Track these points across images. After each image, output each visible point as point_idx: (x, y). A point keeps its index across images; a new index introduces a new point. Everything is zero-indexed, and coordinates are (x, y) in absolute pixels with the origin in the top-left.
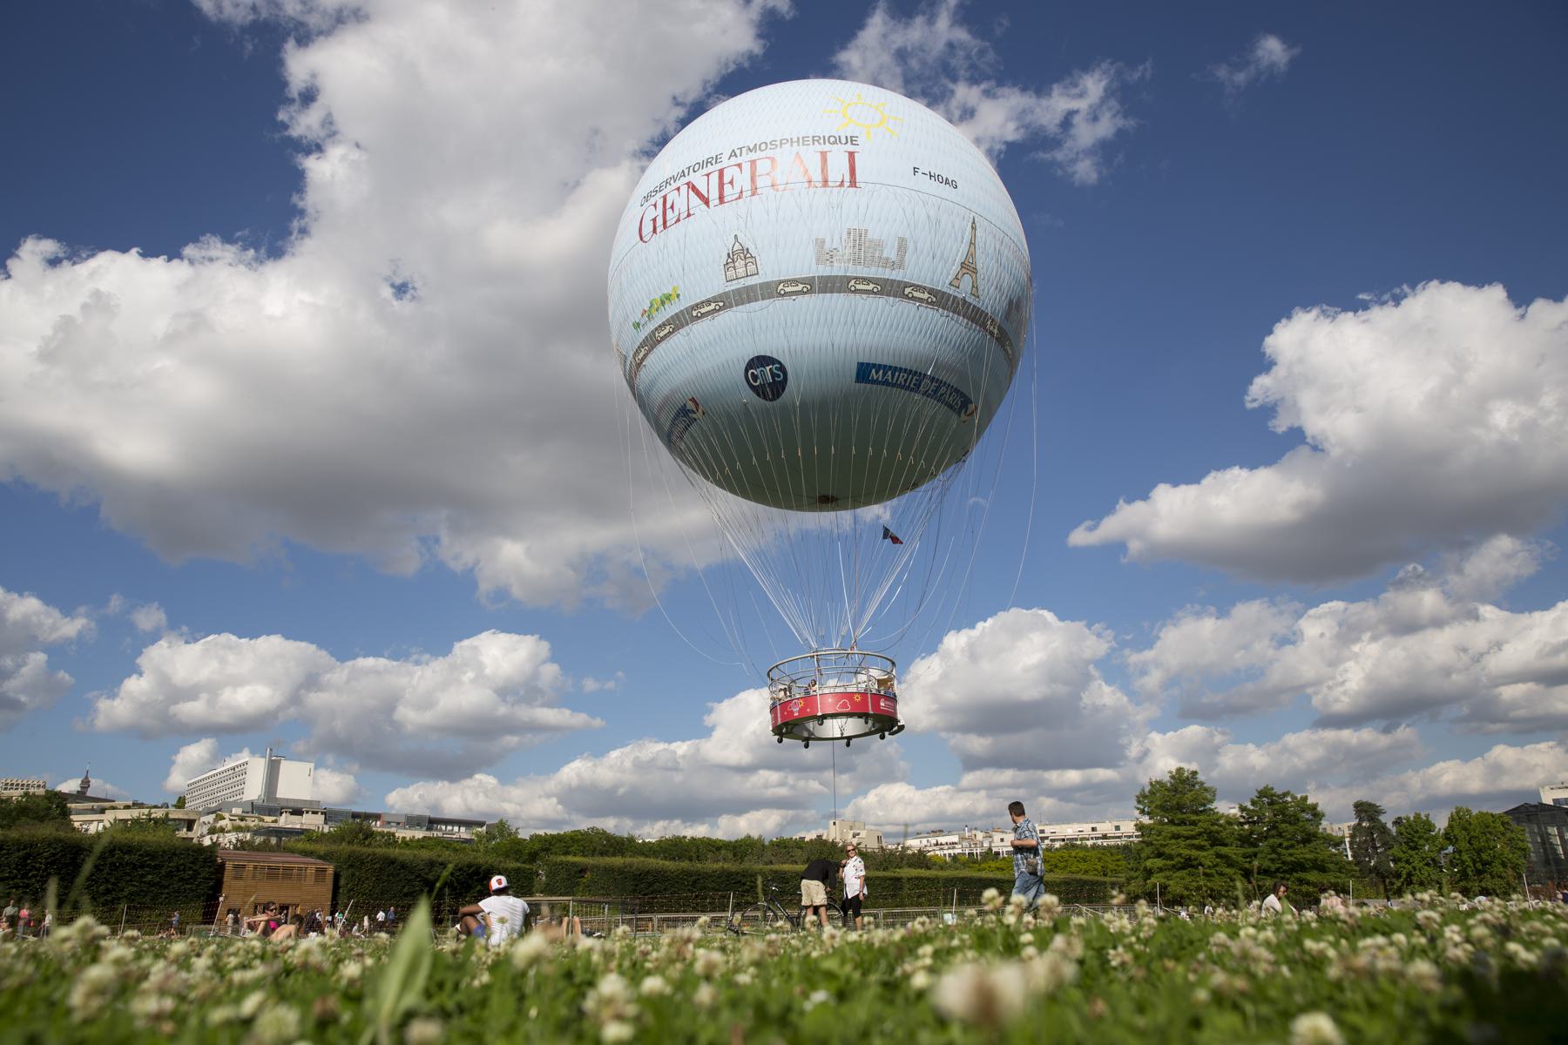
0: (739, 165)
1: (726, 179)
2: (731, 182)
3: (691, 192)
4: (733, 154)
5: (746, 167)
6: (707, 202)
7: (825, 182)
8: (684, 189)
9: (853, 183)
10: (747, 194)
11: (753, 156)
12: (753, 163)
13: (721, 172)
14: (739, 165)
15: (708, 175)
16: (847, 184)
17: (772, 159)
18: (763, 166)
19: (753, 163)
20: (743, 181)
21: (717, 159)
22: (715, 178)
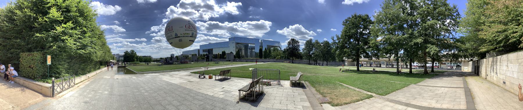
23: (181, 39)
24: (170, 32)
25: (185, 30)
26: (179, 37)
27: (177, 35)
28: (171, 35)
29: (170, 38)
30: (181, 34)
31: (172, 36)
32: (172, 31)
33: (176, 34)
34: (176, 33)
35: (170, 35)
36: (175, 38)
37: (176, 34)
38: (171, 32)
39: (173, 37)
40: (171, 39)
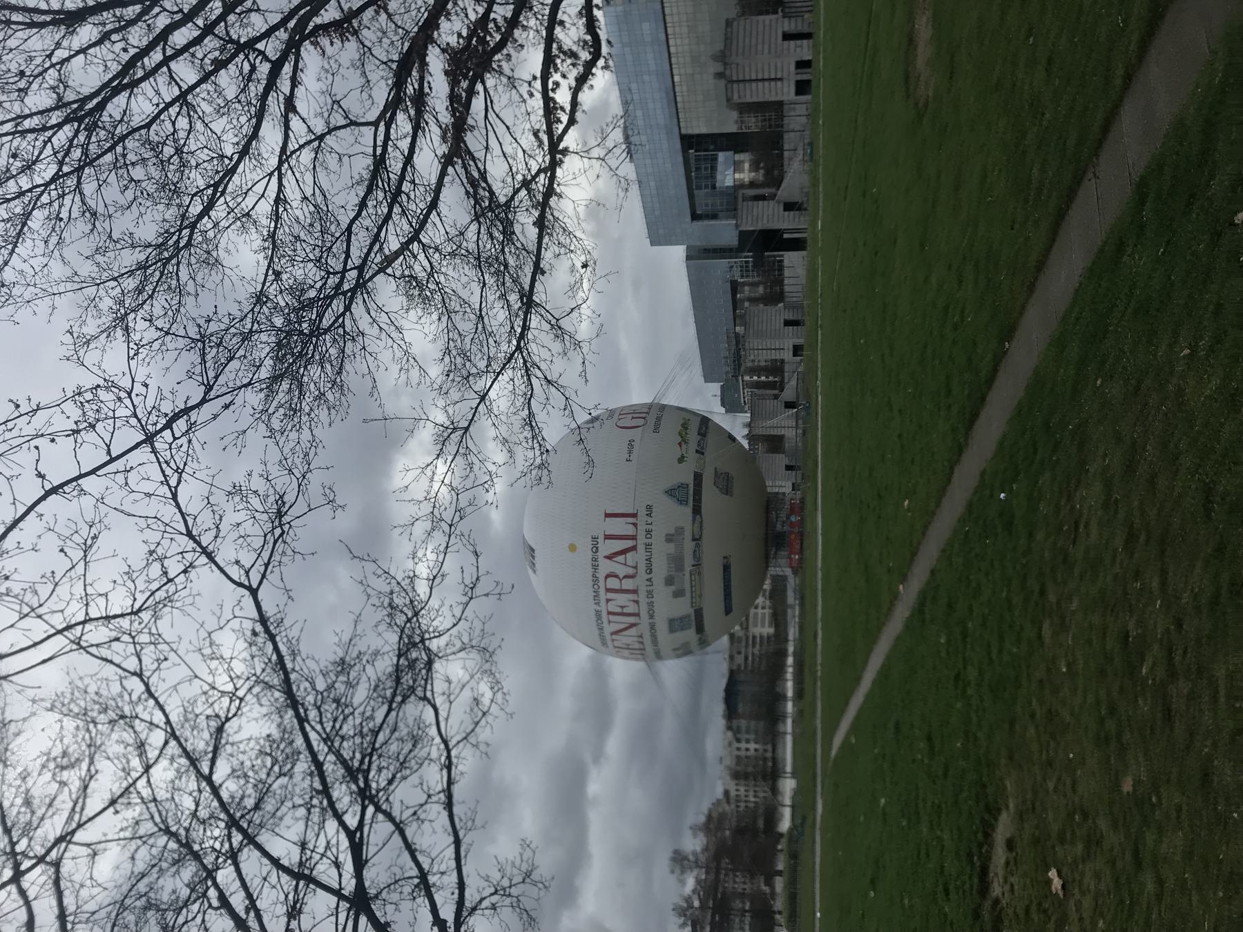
0: (608, 600)
1: (619, 610)
2: (622, 607)
3: (624, 633)
4: (598, 604)
5: (610, 595)
6: (632, 625)
7: (634, 538)
8: (614, 637)
9: (634, 515)
10: (631, 597)
11: (602, 591)
12: (608, 590)
13: (610, 613)
14: (608, 600)
15: (610, 622)
16: (631, 520)
17: (607, 576)
18: (613, 583)
19: (608, 590)
20: (622, 599)
21: (598, 614)
22: (612, 618)
23: (717, 474)
24: (642, 539)
25: (656, 430)
26: (698, 477)
27: (682, 486)
28: (669, 539)
29: (689, 561)
30: (681, 460)
31: (680, 530)
32: (642, 518)
33: (670, 492)
34: (668, 485)
35: (671, 548)
36: (697, 511)
37: (670, 492)
38: (649, 532)
39: (688, 535)
40: (697, 555)
